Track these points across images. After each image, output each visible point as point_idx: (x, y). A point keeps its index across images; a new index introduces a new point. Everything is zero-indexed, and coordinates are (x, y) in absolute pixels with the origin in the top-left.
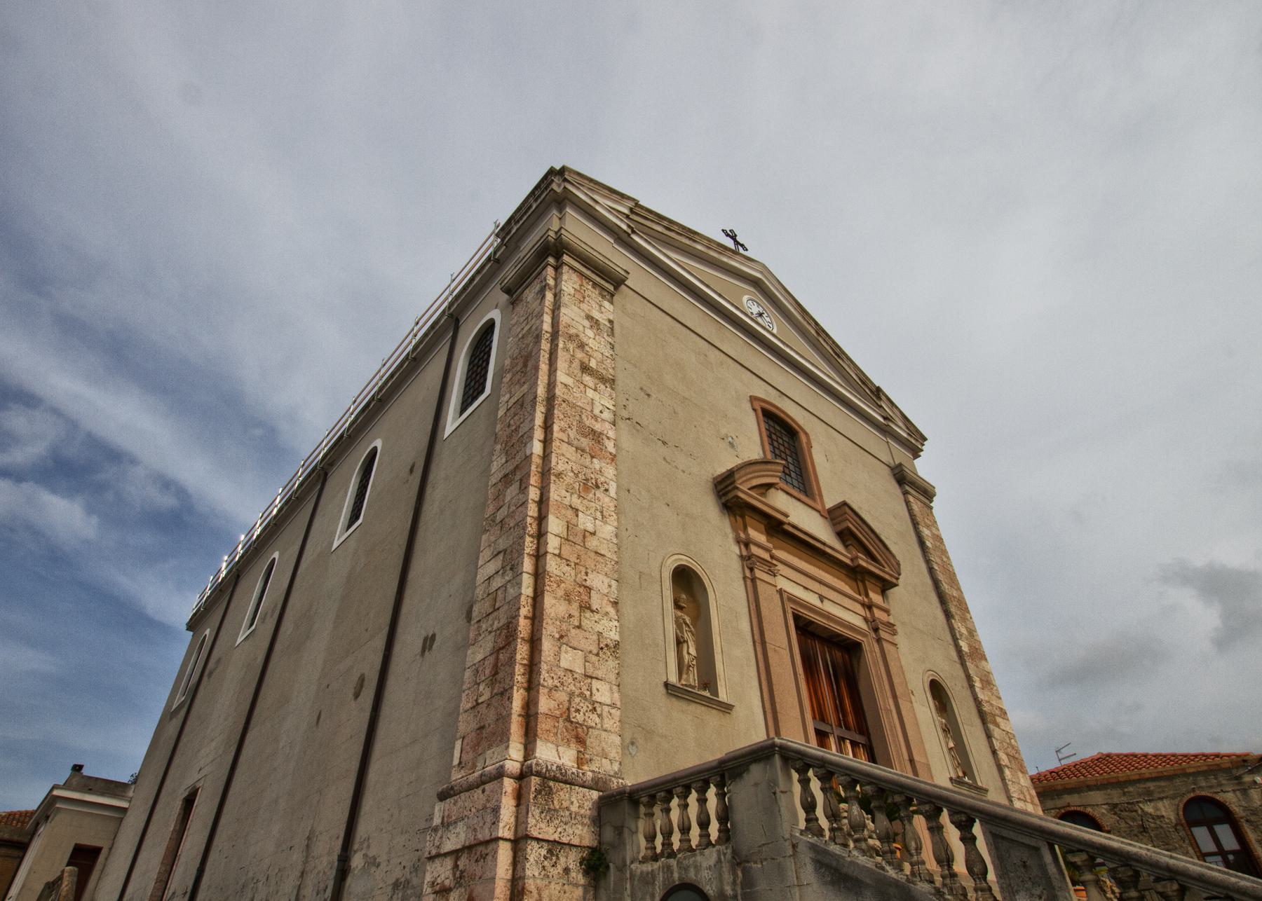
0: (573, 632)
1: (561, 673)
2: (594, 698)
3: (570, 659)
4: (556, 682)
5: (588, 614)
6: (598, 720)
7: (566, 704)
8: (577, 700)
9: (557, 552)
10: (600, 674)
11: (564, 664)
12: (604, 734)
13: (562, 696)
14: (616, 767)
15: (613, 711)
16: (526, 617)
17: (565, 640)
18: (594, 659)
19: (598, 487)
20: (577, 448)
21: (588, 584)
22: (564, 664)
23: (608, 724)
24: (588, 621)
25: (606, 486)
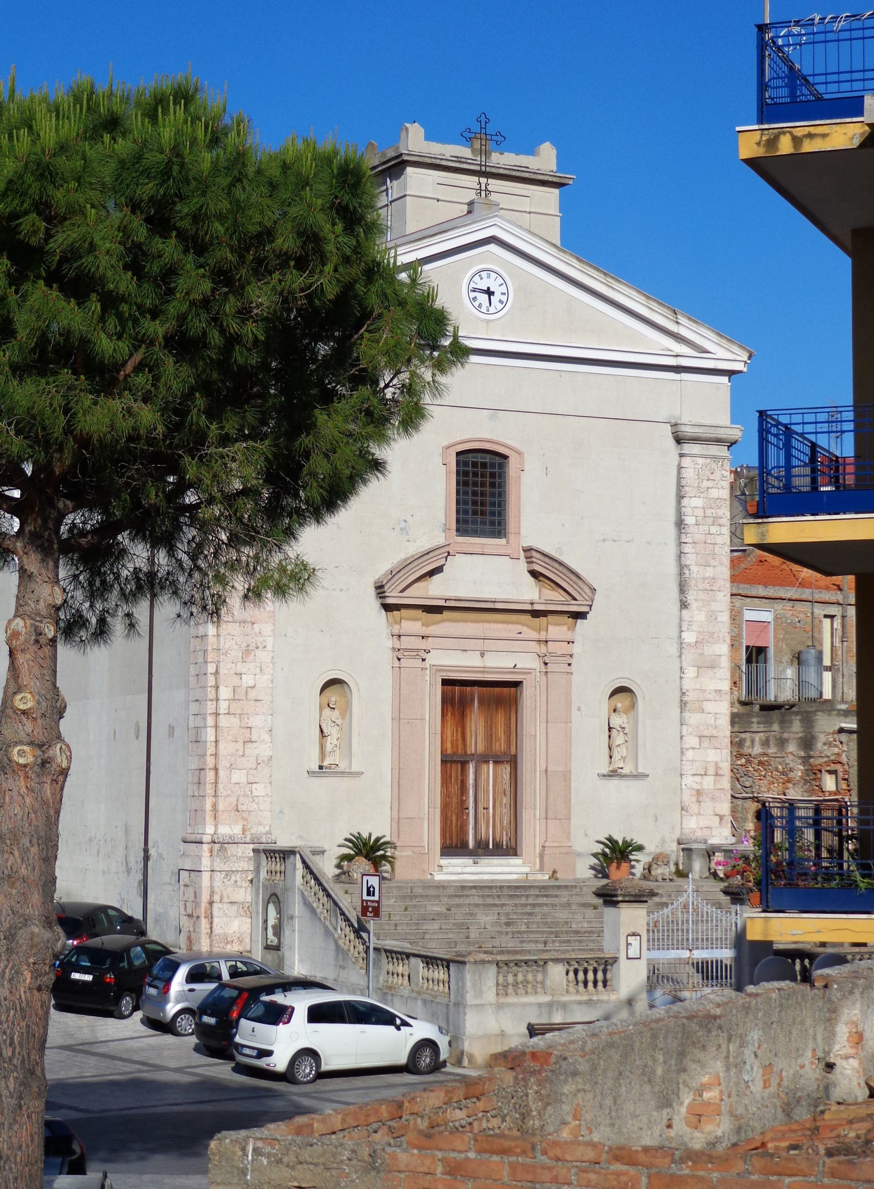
0: (239, 760)
1: (231, 786)
2: (254, 794)
3: (238, 776)
4: (229, 792)
5: (249, 745)
6: (256, 806)
7: (235, 803)
8: (242, 798)
9: (226, 711)
10: (256, 780)
11: (234, 780)
12: (260, 813)
13: (233, 800)
14: (267, 829)
15: (265, 799)
16: (211, 755)
17: (234, 766)
18: (253, 772)
19: (257, 648)
20: (240, 623)
21: (249, 725)
22: (234, 780)
23: (262, 807)
24: (251, 749)
25: (264, 644)
